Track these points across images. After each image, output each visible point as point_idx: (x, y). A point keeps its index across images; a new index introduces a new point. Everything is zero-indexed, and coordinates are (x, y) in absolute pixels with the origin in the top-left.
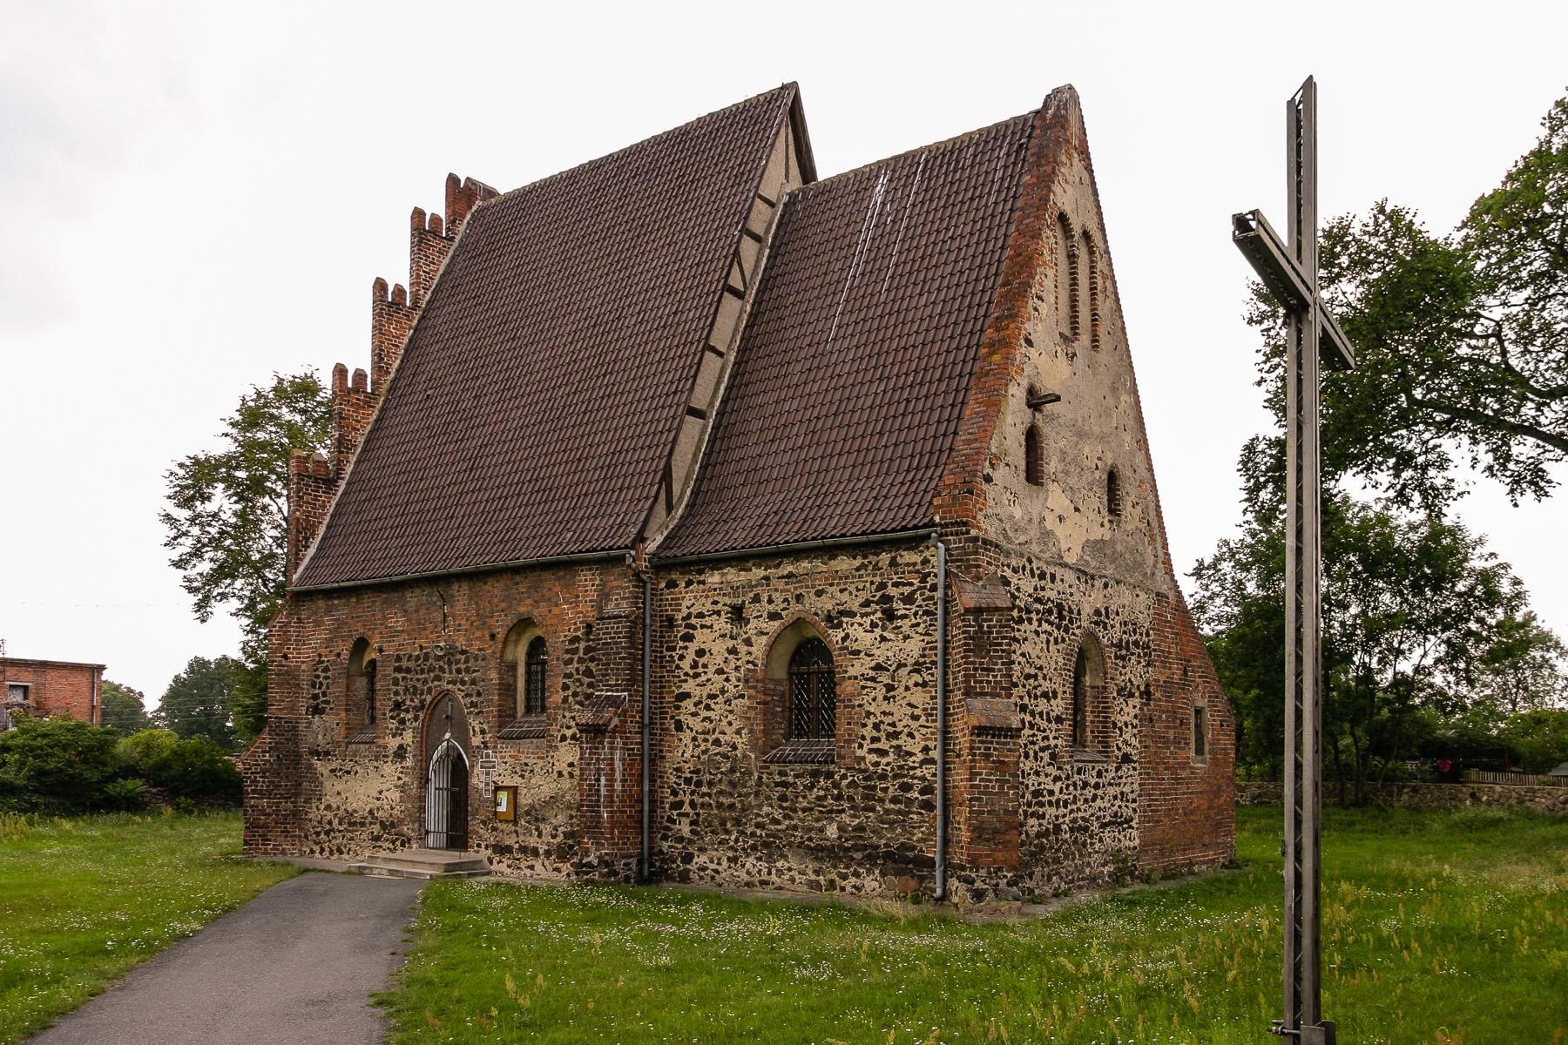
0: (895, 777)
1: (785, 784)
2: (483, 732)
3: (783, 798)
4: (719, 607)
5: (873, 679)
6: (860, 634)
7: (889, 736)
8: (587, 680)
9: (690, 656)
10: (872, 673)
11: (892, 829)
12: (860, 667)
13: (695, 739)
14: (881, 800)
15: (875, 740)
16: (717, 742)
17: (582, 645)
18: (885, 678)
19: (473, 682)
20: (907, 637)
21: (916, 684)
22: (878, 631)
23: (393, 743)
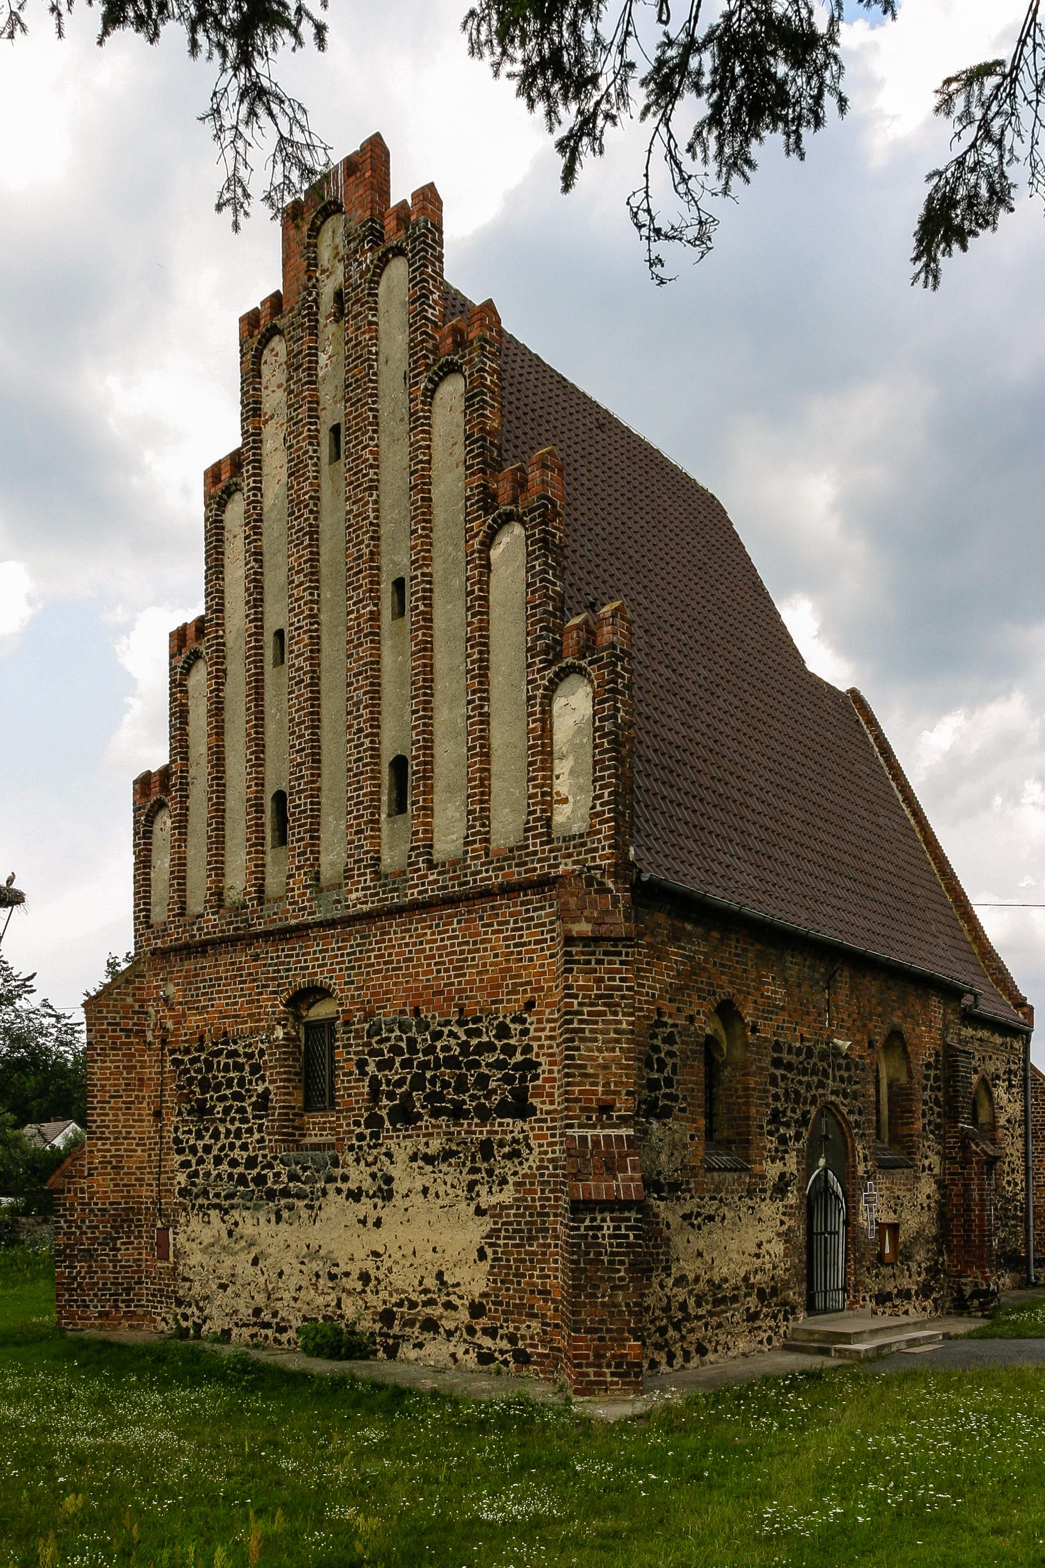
23: (772, 1170)
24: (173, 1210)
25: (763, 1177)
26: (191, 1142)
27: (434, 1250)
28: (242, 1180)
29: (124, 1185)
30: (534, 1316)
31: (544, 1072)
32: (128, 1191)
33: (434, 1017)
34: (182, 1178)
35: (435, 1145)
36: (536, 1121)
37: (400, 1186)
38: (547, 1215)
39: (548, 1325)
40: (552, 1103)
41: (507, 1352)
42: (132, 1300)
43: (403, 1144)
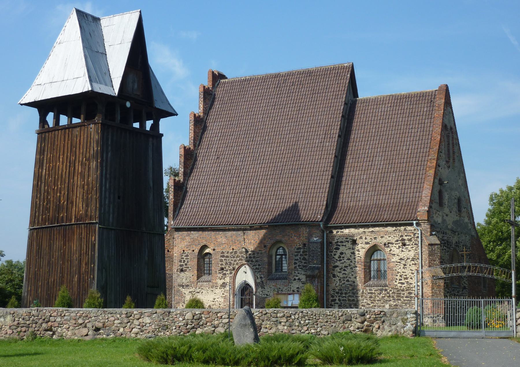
0: (407, 290)
1: (372, 293)
2: (261, 278)
3: (371, 297)
4: (348, 240)
5: (399, 262)
6: (395, 249)
7: (405, 279)
8: (304, 261)
9: (338, 254)
10: (399, 261)
11: (406, 305)
12: (395, 259)
13: (340, 280)
14: (403, 297)
15: (400, 280)
16: (348, 281)
17: (302, 250)
18: (403, 262)
19: (257, 261)
20: (409, 251)
21: (413, 264)
22: (401, 249)
23: (220, 282)
25: (216, 283)
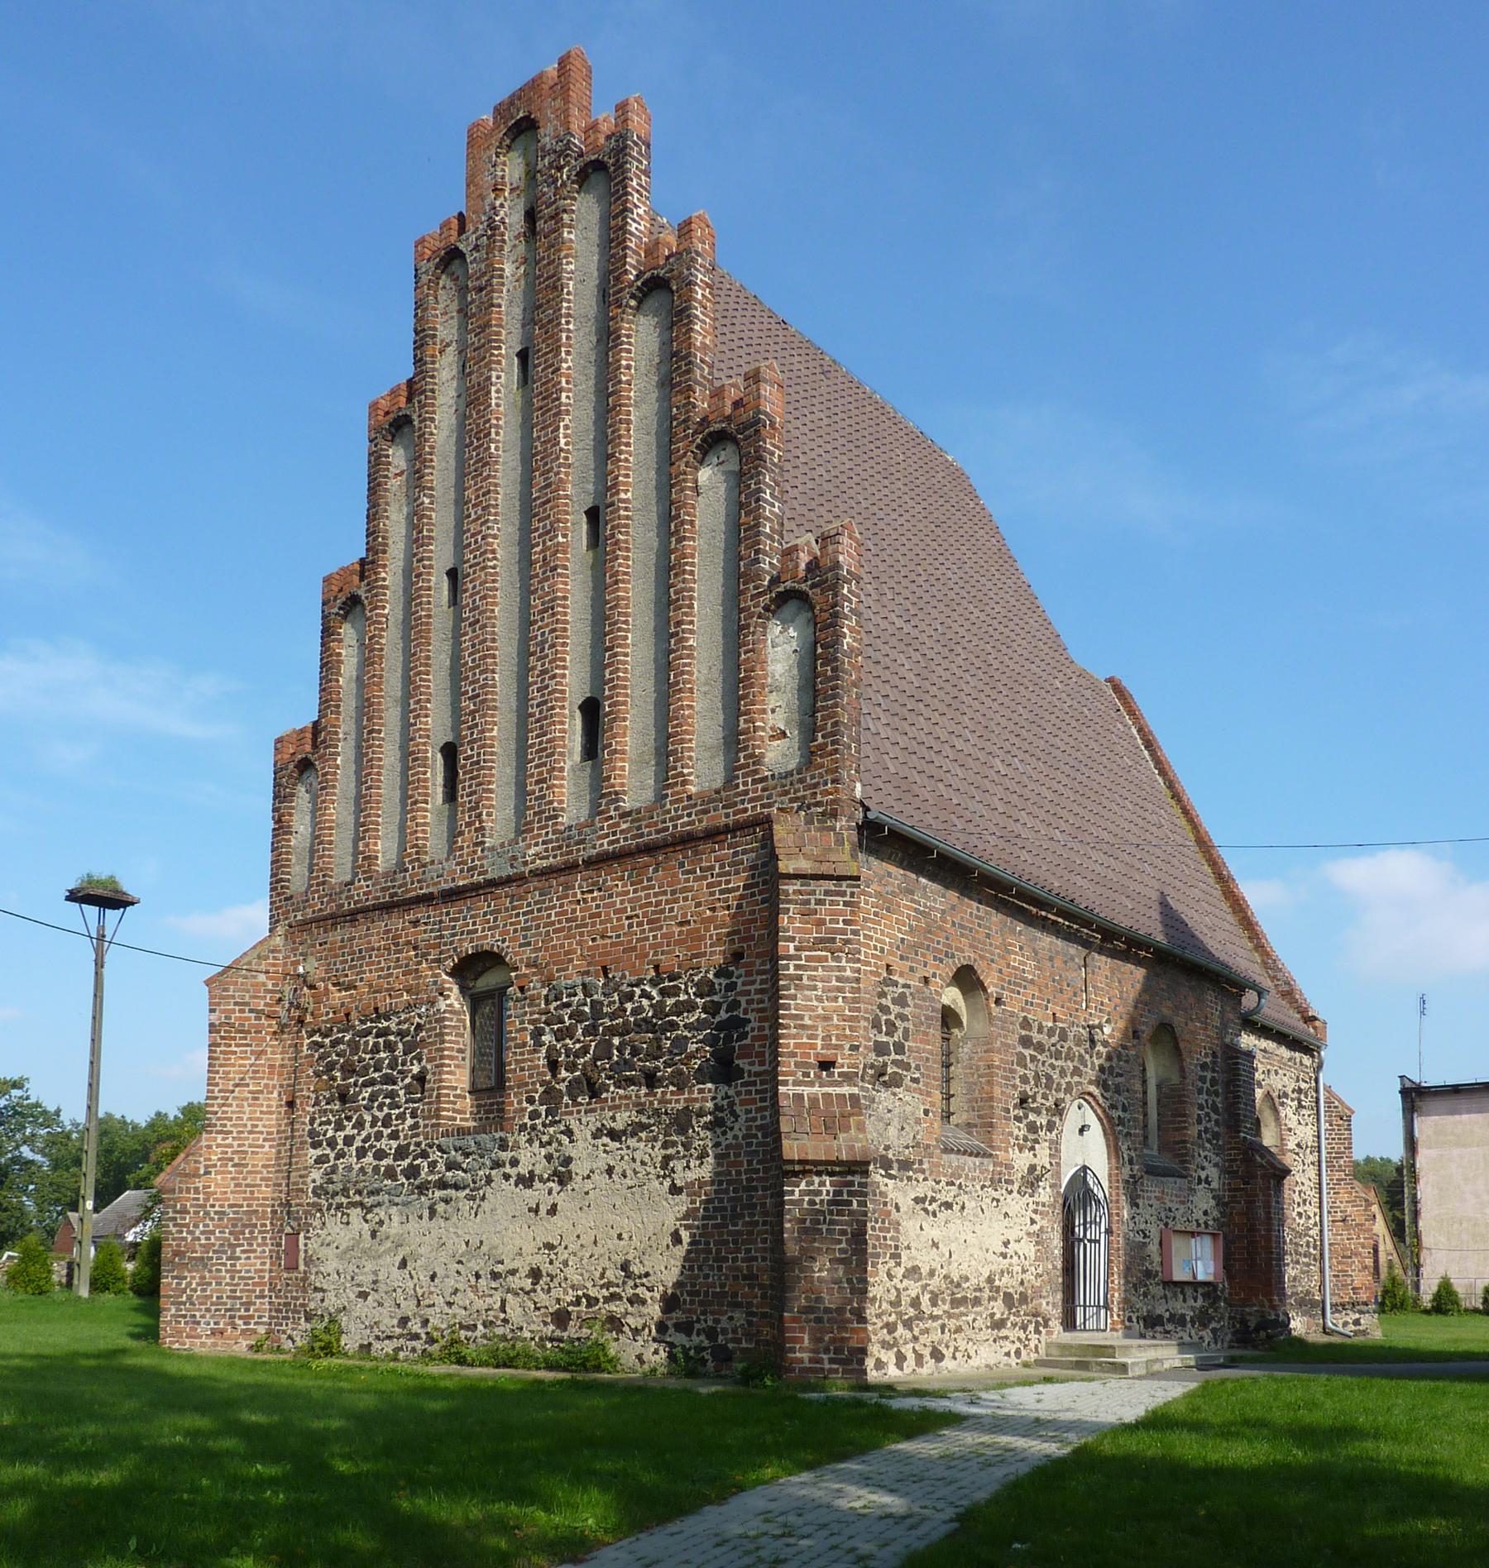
24: (306, 1212)
26: (330, 1134)
27: (620, 1237)
28: (390, 1173)
29: (247, 1186)
30: (738, 1305)
31: (753, 1030)
32: (252, 1192)
33: (624, 977)
34: (316, 1175)
35: (622, 1119)
36: (743, 1085)
37: (579, 1168)
38: (755, 1189)
39: (753, 1314)
40: (762, 1063)
41: (704, 1349)
42: (252, 1317)
43: (584, 1120)
